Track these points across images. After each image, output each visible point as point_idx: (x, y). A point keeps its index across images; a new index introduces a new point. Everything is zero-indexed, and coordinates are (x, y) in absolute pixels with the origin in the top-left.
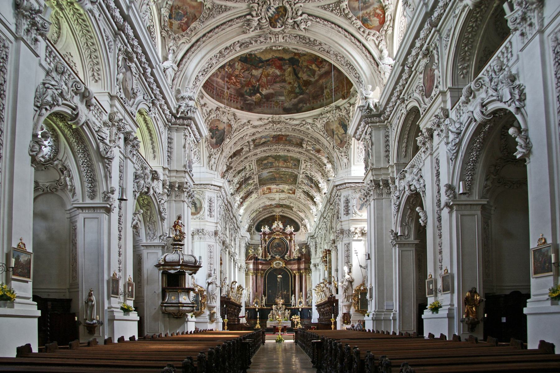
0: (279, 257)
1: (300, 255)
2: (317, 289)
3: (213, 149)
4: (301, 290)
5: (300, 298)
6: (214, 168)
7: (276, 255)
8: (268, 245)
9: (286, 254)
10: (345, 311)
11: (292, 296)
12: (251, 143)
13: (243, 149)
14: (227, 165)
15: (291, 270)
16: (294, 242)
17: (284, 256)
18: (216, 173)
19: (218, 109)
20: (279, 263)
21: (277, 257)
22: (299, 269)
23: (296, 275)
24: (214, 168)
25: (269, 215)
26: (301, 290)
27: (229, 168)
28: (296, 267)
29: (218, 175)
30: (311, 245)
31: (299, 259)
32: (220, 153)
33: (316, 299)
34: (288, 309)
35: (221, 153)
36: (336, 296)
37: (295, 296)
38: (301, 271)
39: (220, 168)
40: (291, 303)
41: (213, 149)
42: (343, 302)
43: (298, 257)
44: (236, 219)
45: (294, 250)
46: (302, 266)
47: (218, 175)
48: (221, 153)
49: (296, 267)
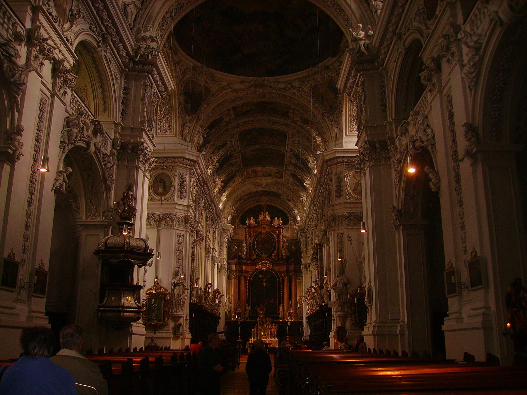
0: (266, 256)
1: (289, 254)
2: (307, 296)
3: (187, 117)
4: (290, 298)
5: (289, 308)
6: (188, 138)
7: (262, 253)
8: (254, 241)
9: (273, 253)
10: (339, 324)
11: (279, 305)
12: (232, 112)
13: (222, 118)
14: (203, 136)
15: (279, 272)
16: (282, 237)
17: (271, 255)
18: (190, 144)
19: (194, 68)
20: (265, 263)
21: (264, 256)
22: (288, 271)
23: (285, 278)
24: (188, 138)
25: (255, 204)
26: (290, 298)
27: (206, 141)
28: (284, 268)
29: (192, 148)
30: (302, 240)
31: (288, 258)
32: (195, 121)
33: (307, 309)
34: (275, 323)
35: (197, 122)
36: (329, 303)
37: (283, 306)
38: (291, 274)
39: (196, 139)
40: (279, 314)
41: (187, 117)
42: (336, 312)
43: (287, 256)
44: (215, 206)
45: (283, 247)
46: (292, 268)
47: (192, 148)
48: (197, 122)
49: (284, 268)
